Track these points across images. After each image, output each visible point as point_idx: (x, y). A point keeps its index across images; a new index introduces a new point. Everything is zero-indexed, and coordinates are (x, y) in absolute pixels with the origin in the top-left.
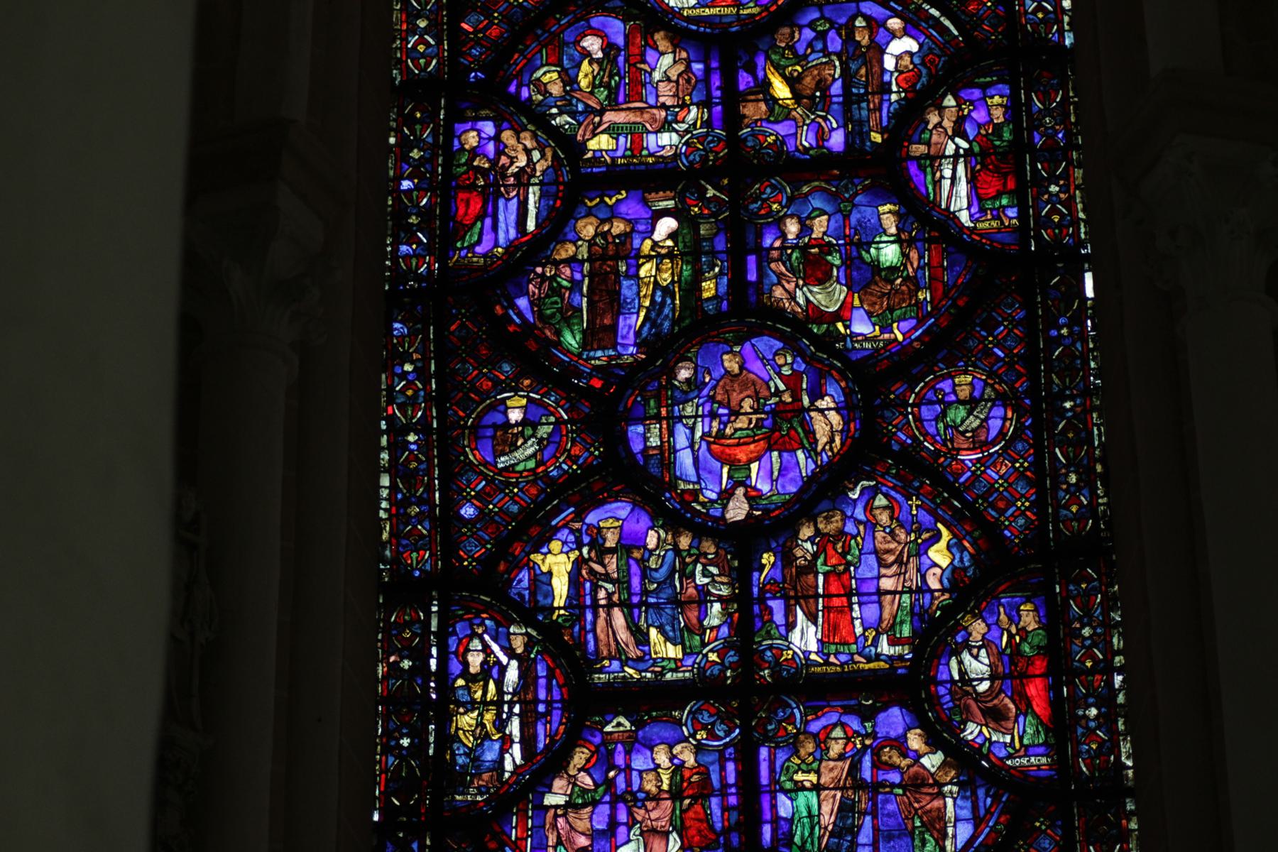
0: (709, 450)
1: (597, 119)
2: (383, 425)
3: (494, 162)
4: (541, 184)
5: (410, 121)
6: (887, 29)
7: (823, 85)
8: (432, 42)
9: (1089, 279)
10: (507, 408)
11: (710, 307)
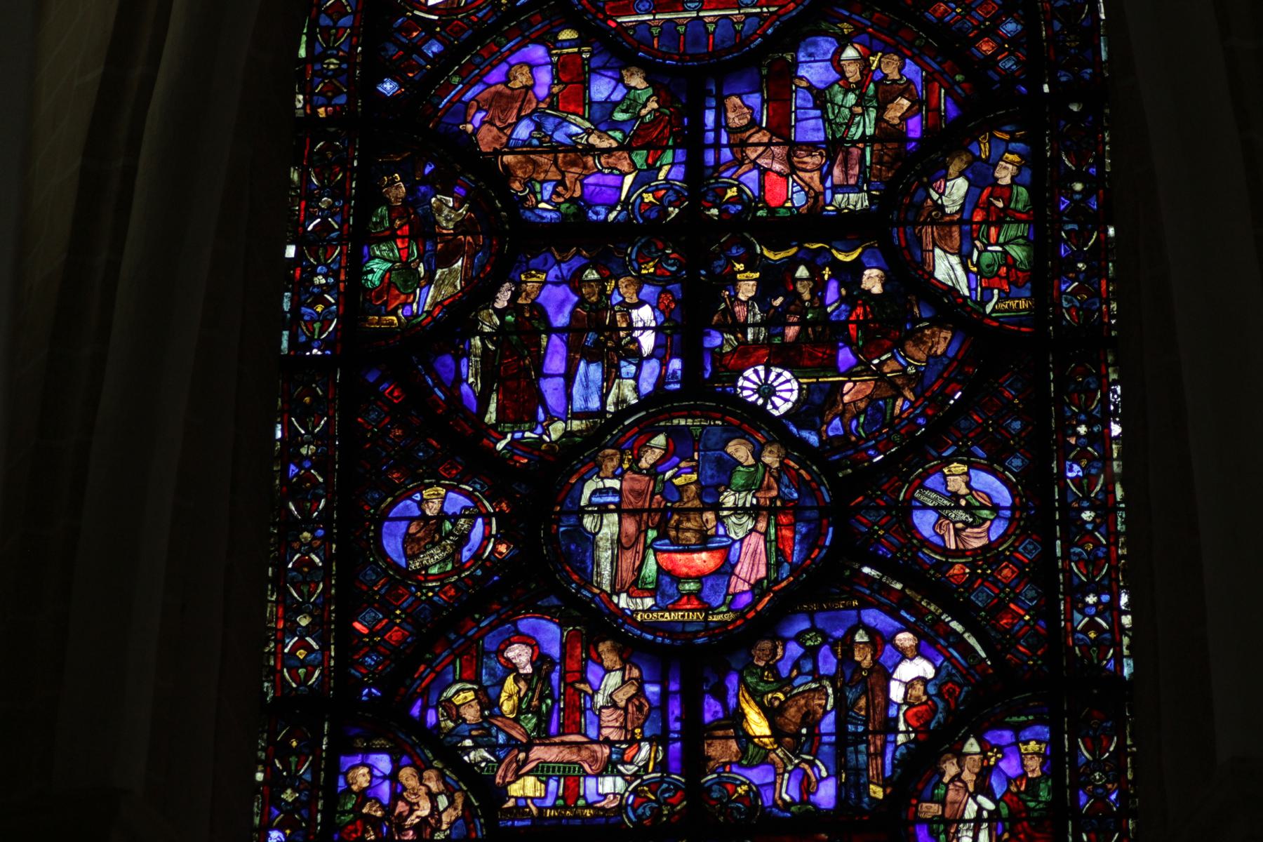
1: (522, 756)
3: (389, 809)
5: (283, 751)
6: (896, 647)
7: (811, 720)
8: (316, 647)
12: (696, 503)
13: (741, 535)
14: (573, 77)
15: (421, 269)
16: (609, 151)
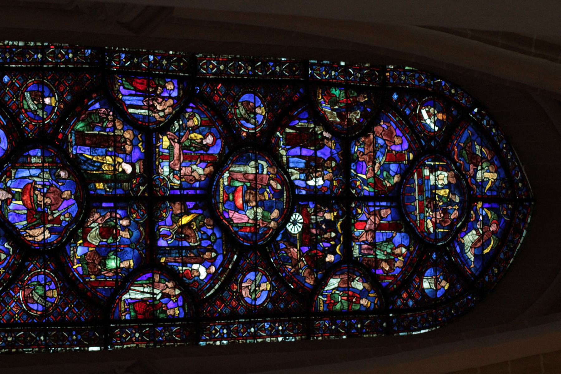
0: (29, 183)
2: (46, 44)
4: (149, 116)
5: (179, 60)
6: (210, 266)
7: (187, 238)
8: (213, 71)
9: (97, 349)
10: (51, 97)
11: (92, 186)
12: (258, 199)
13: (248, 214)
14: (397, 158)
15: (336, 107)
16: (374, 170)
